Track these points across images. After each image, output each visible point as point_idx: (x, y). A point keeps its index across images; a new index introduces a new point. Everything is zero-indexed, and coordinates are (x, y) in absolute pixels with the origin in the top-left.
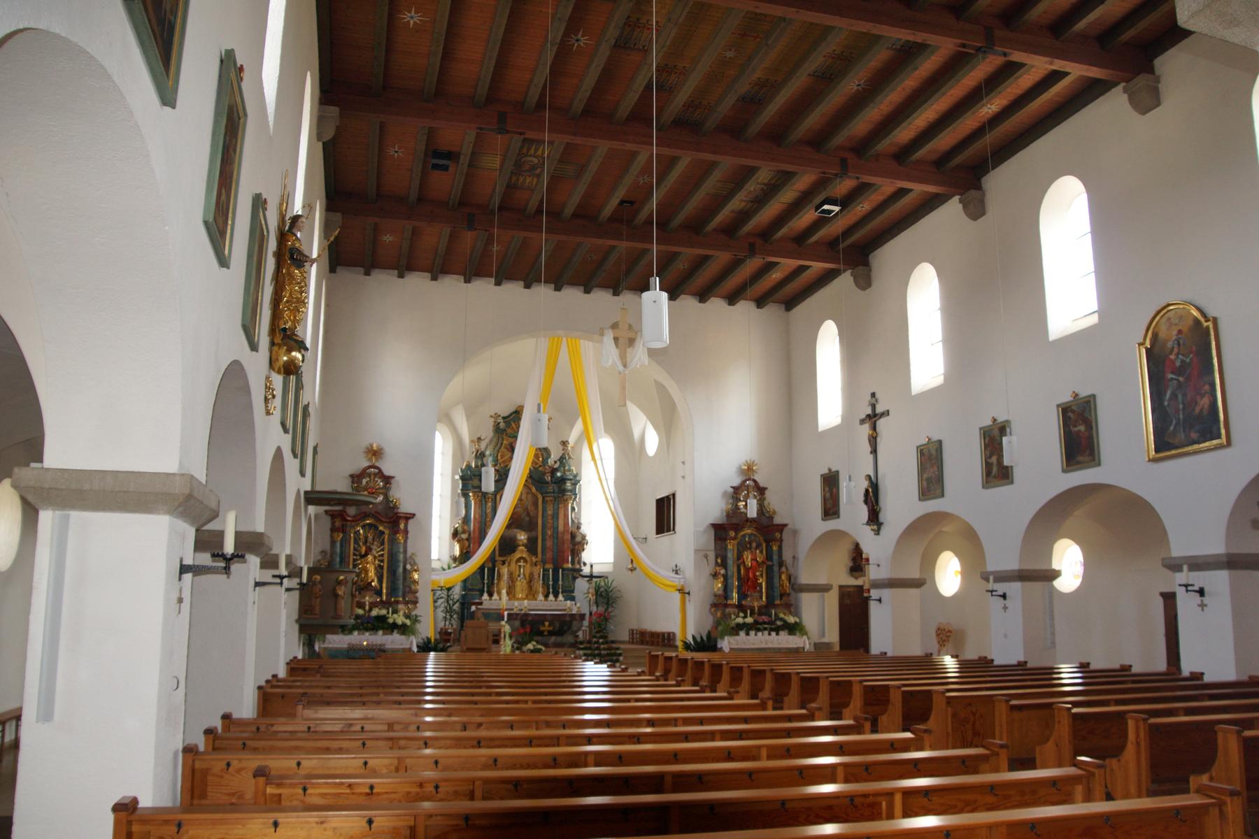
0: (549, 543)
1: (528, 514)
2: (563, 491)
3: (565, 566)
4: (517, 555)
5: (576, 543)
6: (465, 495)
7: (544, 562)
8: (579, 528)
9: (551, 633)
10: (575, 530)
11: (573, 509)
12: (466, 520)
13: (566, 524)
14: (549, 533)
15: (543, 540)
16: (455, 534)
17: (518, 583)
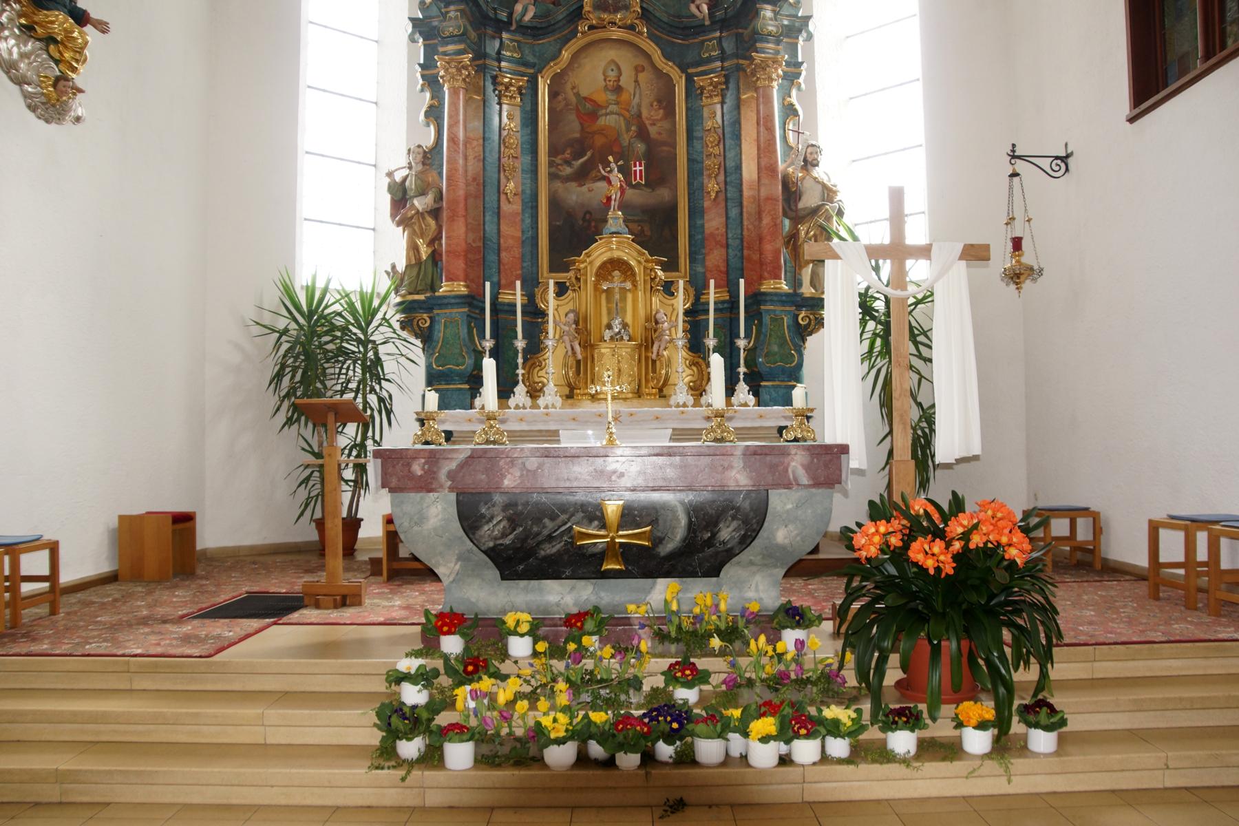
0: (713, 222)
1: (643, 134)
2: (748, 42)
3: (768, 286)
4: (599, 253)
5: (801, 214)
6: (431, 82)
7: (698, 287)
8: (809, 163)
9: (644, 563)
10: (795, 171)
11: (790, 111)
12: (428, 158)
13: (766, 149)
14: (712, 186)
15: (695, 212)
16: (400, 197)
17: (605, 349)
